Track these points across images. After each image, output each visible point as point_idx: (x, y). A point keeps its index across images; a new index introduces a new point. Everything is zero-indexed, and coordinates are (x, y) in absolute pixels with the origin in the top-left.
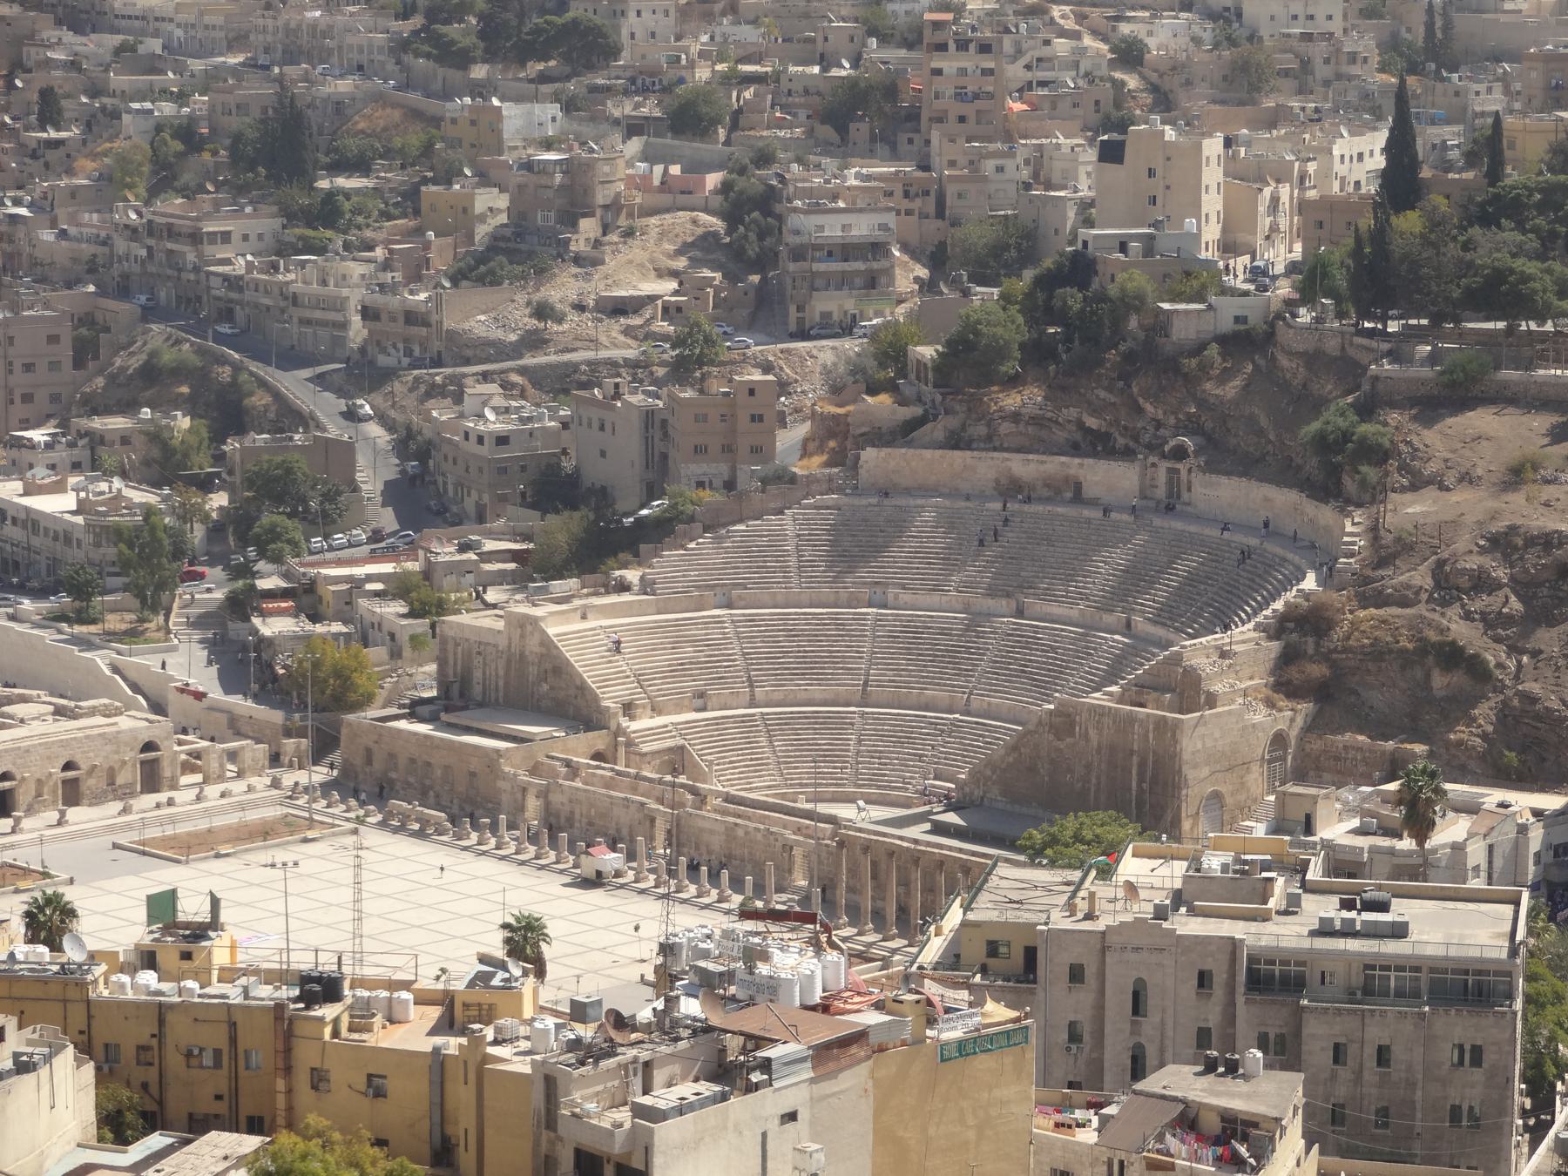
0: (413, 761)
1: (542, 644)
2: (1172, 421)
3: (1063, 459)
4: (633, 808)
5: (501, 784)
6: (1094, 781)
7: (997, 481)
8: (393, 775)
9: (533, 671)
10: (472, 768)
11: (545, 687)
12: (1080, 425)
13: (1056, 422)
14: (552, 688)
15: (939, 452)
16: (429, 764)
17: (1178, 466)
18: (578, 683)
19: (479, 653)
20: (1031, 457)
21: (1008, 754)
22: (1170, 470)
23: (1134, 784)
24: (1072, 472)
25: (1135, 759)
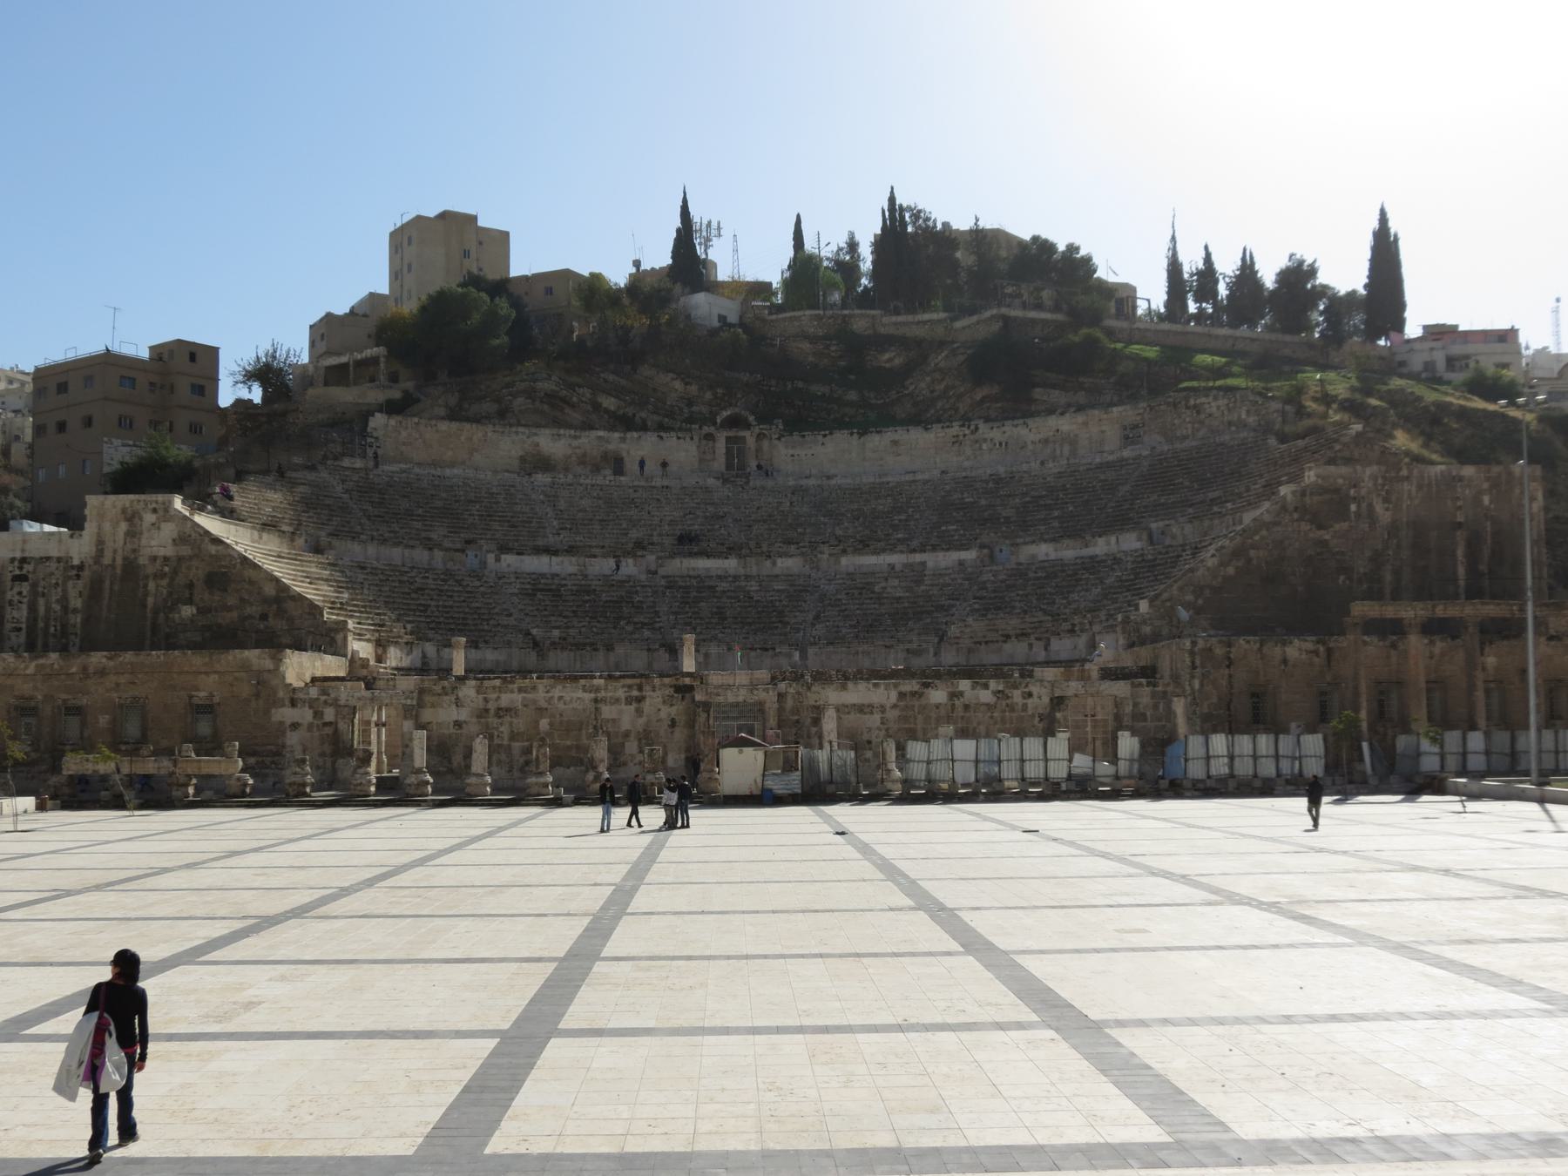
1: (181, 540)
2: (708, 395)
3: (601, 433)
5: (286, 714)
6: (1388, 577)
7: (523, 459)
9: (155, 591)
11: (187, 611)
12: (597, 407)
13: (567, 403)
15: (455, 425)
16: (77, 711)
17: (741, 434)
18: (269, 590)
21: (1222, 564)
23: (1461, 571)
24: (611, 447)
25: (1460, 536)
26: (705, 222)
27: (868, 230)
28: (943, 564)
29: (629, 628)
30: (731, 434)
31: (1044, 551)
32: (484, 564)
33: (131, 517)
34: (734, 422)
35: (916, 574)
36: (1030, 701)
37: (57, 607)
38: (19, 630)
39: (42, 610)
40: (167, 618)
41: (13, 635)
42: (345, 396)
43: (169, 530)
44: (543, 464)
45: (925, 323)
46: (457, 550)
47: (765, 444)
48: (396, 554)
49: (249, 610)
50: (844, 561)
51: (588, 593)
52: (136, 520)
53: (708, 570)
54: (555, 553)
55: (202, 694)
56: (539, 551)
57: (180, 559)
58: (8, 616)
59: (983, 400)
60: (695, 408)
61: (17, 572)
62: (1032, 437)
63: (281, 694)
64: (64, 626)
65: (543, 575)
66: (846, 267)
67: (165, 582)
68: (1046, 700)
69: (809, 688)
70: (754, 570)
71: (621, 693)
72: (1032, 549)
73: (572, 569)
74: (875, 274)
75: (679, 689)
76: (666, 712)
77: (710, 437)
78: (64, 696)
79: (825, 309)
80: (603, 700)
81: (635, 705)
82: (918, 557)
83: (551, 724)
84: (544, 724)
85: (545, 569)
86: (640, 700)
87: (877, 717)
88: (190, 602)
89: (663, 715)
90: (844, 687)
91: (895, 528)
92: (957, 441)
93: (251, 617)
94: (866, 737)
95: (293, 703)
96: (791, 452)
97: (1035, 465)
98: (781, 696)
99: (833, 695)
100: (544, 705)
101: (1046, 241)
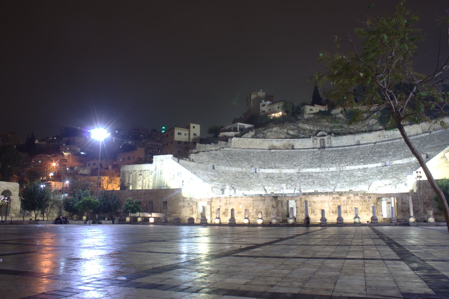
12: (288, 134)
15: (253, 139)
19: (141, 175)
24: (291, 143)
30: (321, 138)
36: (370, 199)
37: (147, 181)
39: (144, 182)
51: (280, 177)
65: (269, 173)
68: (375, 199)
70: (324, 171)
73: (278, 172)
77: (316, 139)
81: (263, 202)
86: (264, 200)
87: (327, 204)
89: (270, 204)
91: (361, 159)
100: (240, 202)
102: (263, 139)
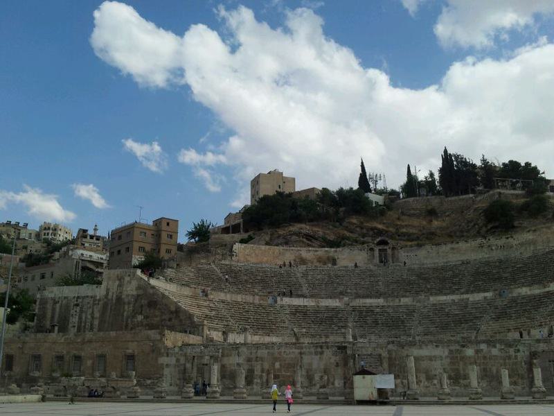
0: (60, 358)
1: (139, 288)
3: (326, 249)
4: (328, 353)
8: (37, 374)
9: (128, 310)
10: (130, 351)
11: (140, 318)
14: (146, 317)
15: (268, 247)
16: (78, 358)
17: (386, 248)
18: (173, 309)
19: (77, 305)
20: (310, 249)
22: (380, 250)
24: (331, 254)
26: (375, 174)
27: (436, 164)
28: (477, 299)
29: (336, 328)
31: (525, 291)
32: (276, 302)
33: (120, 279)
34: (383, 243)
35: (464, 305)
36: (518, 354)
37: (89, 317)
38: (74, 326)
40: (132, 322)
41: (72, 329)
42: (227, 238)
43: (134, 283)
44: (303, 261)
45: (463, 199)
46: (264, 296)
47: (396, 251)
48: (239, 298)
49: (164, 317)
50: (432, 299)
52: (122, 280)
53: (370, 303)
54: (306, 297)
55: (130, 351)
56: (299, 296)
57: (138, 296)
58: (71, 321)
59: (491, 228)
60: (366, 239)
61: (75, 303)
62: (516, 242)
63: (163, 350)
64: (91, 325)
66: (429, 184)
67: (131, 305)
68: (527, 353)
69: (403, 348)
70: (391, 304)
71: (313, 350)
72: (520, 290)
74: (440, 182)
75: (339, 348)
76: (333, 359)
78: (75, 352)
79: (420, 196)
80: (304, 353)
82: (465, 296)
83: (281, 365)
84: (277, 365)
85: (302, 304)
86: (322, 353)
87: (439, 362)
88: (141, 313)
90: (421, 347)
92: (481, 246)
93: (165, 320)
94: (433, 373)
95: (168, 356)
96: (406, 254)
97: (517, 254)
98: (389, 352)
99: (416, 352)
100: (276, 355)
101: (516, 162)
102: (285, 248)
